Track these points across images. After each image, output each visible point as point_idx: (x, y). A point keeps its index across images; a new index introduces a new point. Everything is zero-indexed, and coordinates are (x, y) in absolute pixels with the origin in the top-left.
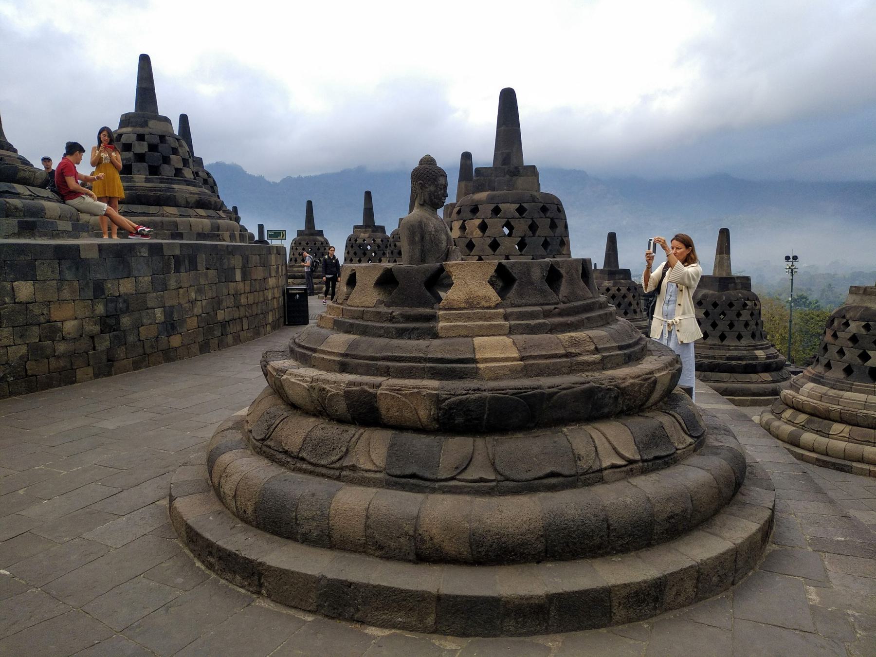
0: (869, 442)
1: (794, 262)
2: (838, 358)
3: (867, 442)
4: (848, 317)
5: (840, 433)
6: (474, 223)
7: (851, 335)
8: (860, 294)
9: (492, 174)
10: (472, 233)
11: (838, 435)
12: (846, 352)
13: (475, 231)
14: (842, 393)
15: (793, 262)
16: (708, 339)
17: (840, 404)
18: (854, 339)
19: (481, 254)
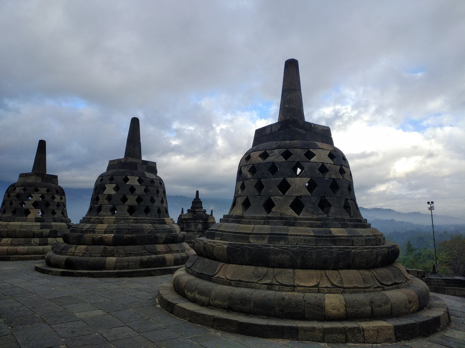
0: (22, 244)
2: (9, 206)
3: (19, 245)
4: (16, 185)
5: (6, 242)
8: (24, 177)
11: (6, 243)
12: (13, 203)
14: (9, 223)
17: (8, 228)
18: (18, 196)
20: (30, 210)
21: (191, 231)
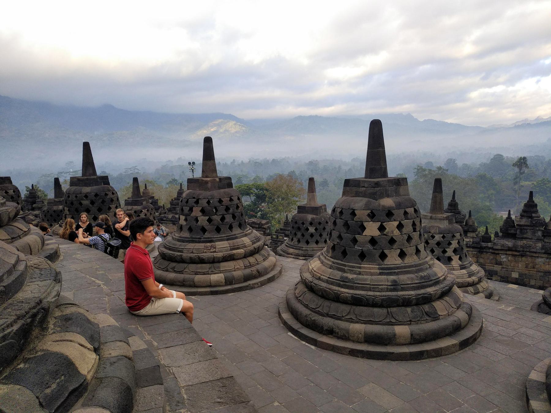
4: (432, 231)
7: (436, 242)
10: (392, 232)
13: (395, 230)
15: (192, 165)
16: (319, 244)
18: (438, 244)
19: (402, 247)
20: (452, 257)
21: (526, 238)
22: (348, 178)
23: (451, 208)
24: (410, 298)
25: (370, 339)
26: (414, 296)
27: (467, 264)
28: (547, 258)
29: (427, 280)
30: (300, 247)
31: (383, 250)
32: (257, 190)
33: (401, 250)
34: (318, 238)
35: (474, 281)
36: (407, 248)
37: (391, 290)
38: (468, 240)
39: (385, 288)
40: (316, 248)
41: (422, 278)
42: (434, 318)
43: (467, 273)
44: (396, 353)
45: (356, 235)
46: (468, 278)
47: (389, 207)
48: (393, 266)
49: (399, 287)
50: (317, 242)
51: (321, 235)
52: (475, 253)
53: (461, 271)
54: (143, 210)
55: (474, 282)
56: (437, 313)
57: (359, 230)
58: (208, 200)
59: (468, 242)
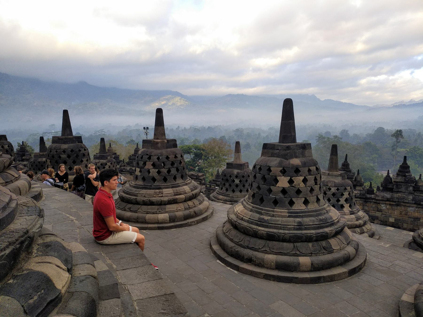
1: (147, 130)
4: (329, 185)
6: (300, 179)
7: (332, 193)
9: (295, 148)
10: (299, 185)
12: (331, 200)
18: (334, 194)
19: (306, 196)
20: (344, 205)
21: (401, 192)
22: (266, 142)
23: (344, 167)
24: (312, 236)
25: (280, 267)
26: (314, 234)
27: (355, 211)
28: (416, 208)
29: (324, 222)
30: (228, 194)
31: (291, 198)
32: (196, 149)
33: (306, 198)
34: (242, 188)
35: (360, 224)
36: (309, 197)
37: (297, 229)
38: (356, 192)
39: (292, 227)
40: (240, 195)
41: (321, 220)
42: (329, 251)
43: (355, 217)
44: (300, 278)
45: (271, 187)
46: (355, 221)
47: (297, 166)
48: (299, 210)
49: (303, 227)
50: (241, 191)
51: (244, 186)
52: (362, 202)
53: (351, 216)
54: (108, 163)
55: (360, 225)
56: (332, 248)
57: (274, 183)
58: (158, 156)
59: (356, 193)
